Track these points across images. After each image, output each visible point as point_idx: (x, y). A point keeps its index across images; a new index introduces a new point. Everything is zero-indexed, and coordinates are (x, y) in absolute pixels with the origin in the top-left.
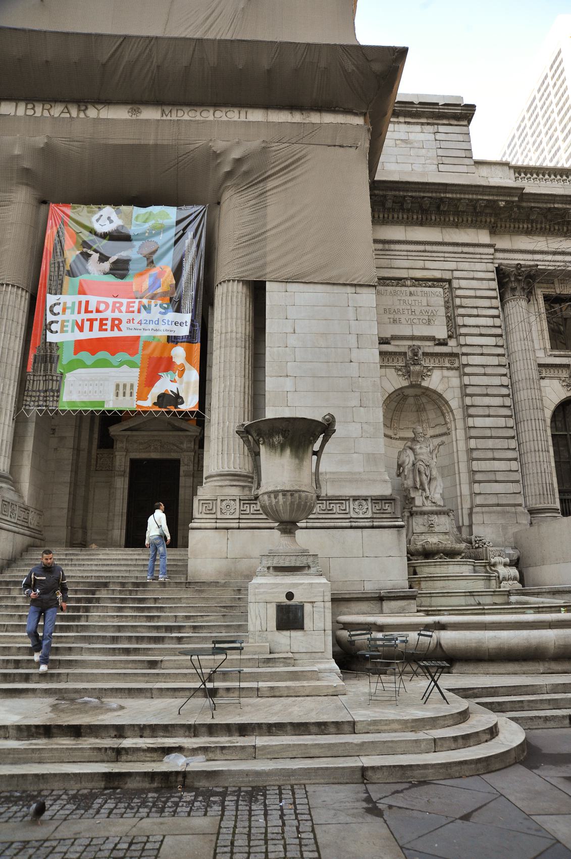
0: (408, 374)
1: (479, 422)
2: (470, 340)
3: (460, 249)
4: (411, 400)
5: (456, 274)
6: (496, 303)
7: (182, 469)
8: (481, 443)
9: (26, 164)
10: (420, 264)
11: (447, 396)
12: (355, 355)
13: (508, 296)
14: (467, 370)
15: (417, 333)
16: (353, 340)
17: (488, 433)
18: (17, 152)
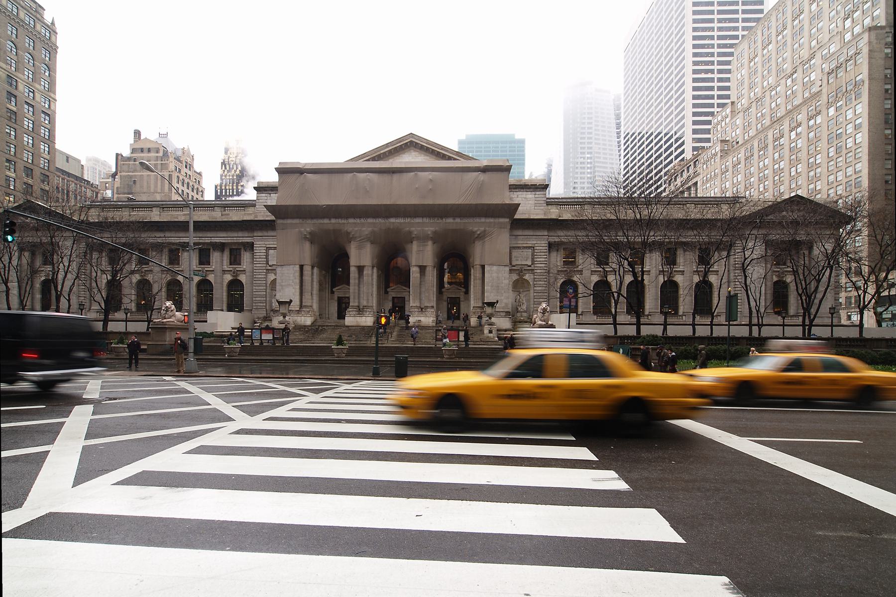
0: (519, 275)
1: (537, 288)
2: (537, 265)
3: (538, 237)
4: (520, 281)
5: (536, 245)
6: (547, 254)
7: (461, 300)
8: (537, 294)
9: (431, 236)
10: (526, 242)
11: (529, 281)
12: (504, 282)
13: (551, 250)
14: (536, 274)
15: (523, 264)
16: (503, 278)
17: (539, 291)
18: (429, 233)
